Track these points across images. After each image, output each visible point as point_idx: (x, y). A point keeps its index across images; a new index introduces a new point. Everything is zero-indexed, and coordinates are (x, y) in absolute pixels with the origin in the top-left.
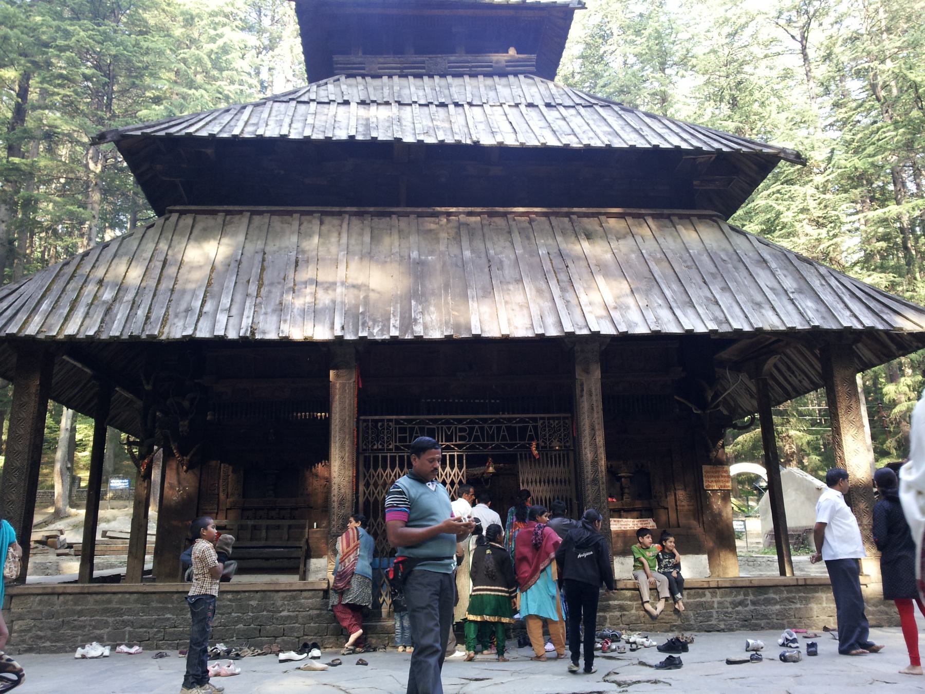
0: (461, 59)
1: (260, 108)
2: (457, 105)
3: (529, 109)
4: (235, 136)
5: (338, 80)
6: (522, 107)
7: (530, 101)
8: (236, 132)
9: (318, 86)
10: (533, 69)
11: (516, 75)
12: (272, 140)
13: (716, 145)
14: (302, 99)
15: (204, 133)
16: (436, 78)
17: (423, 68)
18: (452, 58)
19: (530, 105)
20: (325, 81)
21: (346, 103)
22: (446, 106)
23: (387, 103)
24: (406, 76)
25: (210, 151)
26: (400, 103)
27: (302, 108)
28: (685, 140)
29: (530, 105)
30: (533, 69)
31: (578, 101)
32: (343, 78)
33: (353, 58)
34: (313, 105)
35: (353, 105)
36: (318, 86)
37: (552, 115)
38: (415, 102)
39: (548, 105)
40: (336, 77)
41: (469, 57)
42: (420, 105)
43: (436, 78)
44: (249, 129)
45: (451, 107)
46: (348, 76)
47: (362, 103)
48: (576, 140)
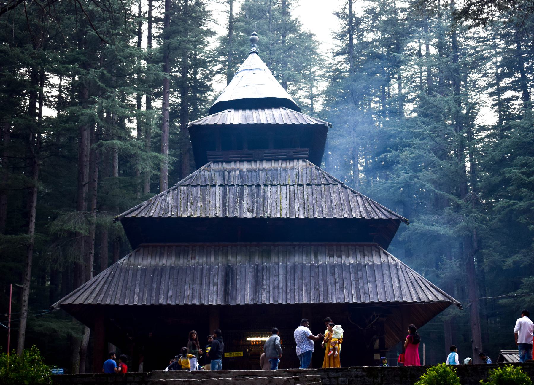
5: (210, 165)
6: (296, 186)
10: (307, 156)
11: (298, 159)
15: (156, 216)
17: (252, 157)
18: (266, 151)
21: (214, 186)
22: (261, 186)
23: (233, 185)
28: (360, 212)
30: (307, 156)
31: (324, 181)
32: (212, 165)
34: (199, 188)
35: (217, 187)
39: (308, 185)
40: (209, 163)
42: (248, 186)
43: (258, 162)
46: (214, 162)
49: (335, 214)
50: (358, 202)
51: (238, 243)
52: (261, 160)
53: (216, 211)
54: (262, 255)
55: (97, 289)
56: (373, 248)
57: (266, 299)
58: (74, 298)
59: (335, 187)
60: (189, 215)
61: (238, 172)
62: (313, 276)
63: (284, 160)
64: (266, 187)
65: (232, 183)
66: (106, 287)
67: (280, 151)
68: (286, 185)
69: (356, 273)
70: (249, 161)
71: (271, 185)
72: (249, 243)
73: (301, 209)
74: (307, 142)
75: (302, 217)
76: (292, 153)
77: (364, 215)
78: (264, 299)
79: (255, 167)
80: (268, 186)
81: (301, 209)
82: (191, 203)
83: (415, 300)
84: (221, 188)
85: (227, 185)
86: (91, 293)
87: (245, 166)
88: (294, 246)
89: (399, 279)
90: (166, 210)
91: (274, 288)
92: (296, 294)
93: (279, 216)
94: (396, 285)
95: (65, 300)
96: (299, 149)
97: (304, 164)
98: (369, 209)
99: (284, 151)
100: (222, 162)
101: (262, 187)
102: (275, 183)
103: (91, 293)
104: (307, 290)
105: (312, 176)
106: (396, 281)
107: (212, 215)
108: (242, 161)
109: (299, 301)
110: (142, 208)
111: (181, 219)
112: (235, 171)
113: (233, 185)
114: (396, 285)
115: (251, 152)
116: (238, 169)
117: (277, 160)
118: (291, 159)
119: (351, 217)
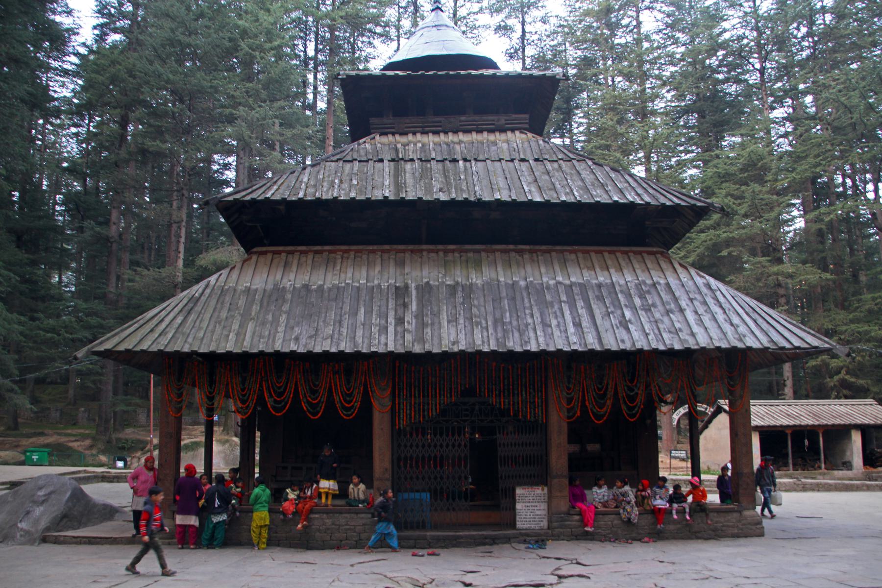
0: (470, 119)
1: (316, 169)
2: (465, 160)
3: (522, 164)
4: (300, 199)
6: (516, 162)
7: (522, 157)
8: (301, 195)
9: (359, 145)
10: (527, 126)
12: (327, 201)
13: (663, 200)
14: (349, 158)
15: (277, 197)
16: (450, 134)
17: (440, 126)
18: (463, 118)
19: (523, 160)
20: (363, 140)
21: (381, 160)
22: (458, 161)
24: (427, 133)
25: (282, 207)
26: (420, 160)
27: (348, 166)
29: (523, 160)
32: (378, 137)
33: (385, 120)
34: (356, 163)
35: (386, 162)
36: (359, 145)
37: (538, 168)
38: (433, 159)
39: (536, 160)
40: (372, 136)
41: (477, 118)
43: (450, 134)
44: (311, 190)
45: (461, 162)
47: (393, 160)
48: (555, 195)
49: (596, 196)
50: (628, 182)
51: (424, 247)
52: (455, 132)
53: (384, 190)
54: (467, 267)
55: (163, 325)
56: (658, 256)
57: (483, 342)
58: (116, 340)
59: (583, 165)
60: (335, 195)
61: (419, 145)
62: (564, 302)
63: (491, 131)
64: (468, 164)
65: (411, 157)
66: (179, 320)
67: (484, 118)
68: (500, 160)
69: (642, 297)
70: (436, 133)
71: (476, 160)
72: (440, 247)
73: (533, 189)
74: (531, 101)
75: (538, 199)
76: (503, 122)
77: (647, 199)
78: (479, 342)
79: (446, 140)
80: (470, 161)
81: (533, 189)
82: (341, 182)
83: (767, 344)
84: (392, 163)
85: (402, 159)
86: (152, 331)
87: (431, 140)
88: (520, 252)
89: (721, 306)
90: (295, 189)
91: (495, 322)
92: (538, 333)
93: (497, 196)
94: (720, 317)
95: (101, 343)
96: (514, 116)
97: (524, 136)
98: (651, 191)
99: (490, 118)
100: (393, 134)
101: (461, 162)
102: (481, 157)
103: (152, 331)
104: (558, 325)
105: (540, 150)
106: (716, 309)
107: (378, 195)
108: (424, 133)
109: (547, 345)
110: (254, 188)
111: (319, 202)
112: (415, 144)
113: (412, 160)
114: (720, 317)
115: (437, 119)
116: (419, 142)
117: (480, 131)
118: (503, 130)
119: (625, 201)
